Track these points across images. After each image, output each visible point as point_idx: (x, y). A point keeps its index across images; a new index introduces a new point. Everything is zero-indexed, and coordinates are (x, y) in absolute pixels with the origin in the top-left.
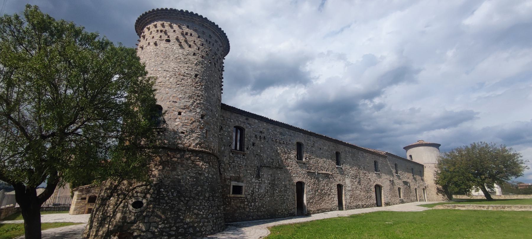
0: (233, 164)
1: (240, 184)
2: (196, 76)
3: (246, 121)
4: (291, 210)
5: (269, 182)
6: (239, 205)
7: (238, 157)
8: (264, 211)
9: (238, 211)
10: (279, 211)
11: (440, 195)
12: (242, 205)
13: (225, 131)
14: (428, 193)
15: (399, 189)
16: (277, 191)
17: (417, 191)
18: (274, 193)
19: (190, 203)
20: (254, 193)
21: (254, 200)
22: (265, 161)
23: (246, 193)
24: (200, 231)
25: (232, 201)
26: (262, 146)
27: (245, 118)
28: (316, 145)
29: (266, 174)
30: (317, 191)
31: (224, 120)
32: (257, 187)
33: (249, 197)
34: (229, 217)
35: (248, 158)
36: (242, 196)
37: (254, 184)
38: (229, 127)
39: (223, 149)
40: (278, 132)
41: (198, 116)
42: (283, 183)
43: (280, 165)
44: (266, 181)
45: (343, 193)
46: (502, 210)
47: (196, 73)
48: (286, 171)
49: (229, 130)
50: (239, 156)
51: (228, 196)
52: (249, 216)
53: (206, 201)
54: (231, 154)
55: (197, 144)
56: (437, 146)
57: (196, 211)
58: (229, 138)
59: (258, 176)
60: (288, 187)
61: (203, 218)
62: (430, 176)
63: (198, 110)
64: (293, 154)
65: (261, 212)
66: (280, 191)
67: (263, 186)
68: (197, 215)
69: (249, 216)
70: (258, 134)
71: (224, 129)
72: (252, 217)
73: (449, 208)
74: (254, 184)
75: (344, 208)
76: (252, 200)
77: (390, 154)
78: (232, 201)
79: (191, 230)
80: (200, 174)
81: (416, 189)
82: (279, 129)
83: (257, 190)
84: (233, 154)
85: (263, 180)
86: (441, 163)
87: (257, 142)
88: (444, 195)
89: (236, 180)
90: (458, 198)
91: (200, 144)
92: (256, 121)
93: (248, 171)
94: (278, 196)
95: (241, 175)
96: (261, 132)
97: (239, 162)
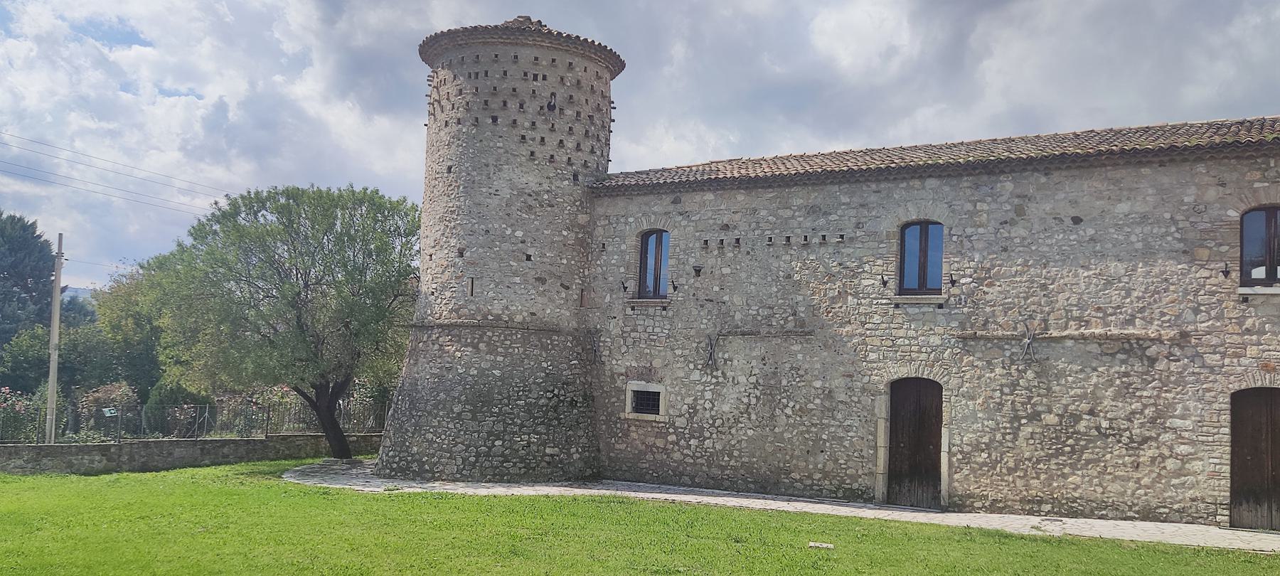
0: (633, 335)
1: (653, 387)
2: (450, 168)
3: (671, 208)
4: (854, 478)
5: (753, 379)
6: (650, 440)
7: (647, 315)
8: (734, 468)
9: (649, 457)
10: (796, 475)
12: (660, 443)
13: (613, 253)
16: (788, 411)
18: (773, 417)
19: (423, 420)
20: (696, 412)
21: (698, 433)
22: (738, 316)
23: (671, 412)
24: (431, 471)
25: (633, 428)
26: (726, 271)
27: (668, 199)
28: (1032, 209)
29: (742, 361)
30: (1035, 417)
31: (610, 223)
32: (708, 395)
33: (680, 422)
34: (624, 468)
35: (677, 314)
36: (658, 418)
37: (700, 387)
38: (623, 240)
39: (608, 299)
40: (799, 209)
41: (453, 255)
42: (818, 384)
43: (803, 324)
44: (742, 379)
47: (450, 163)
48: (834, 344)
49: (623, 247)
50: (651, 311)
51: (622, 415)
52: (682, 474)
53: (453, 419)
54: (629, 311)
55: (451, 311)
57: (430, 436)
58: (622, 270)
59: (711, 364)
60: (842, 397)
61: (442, 449)
63: (453, 242)
64: (877, 273)
65: (723, 468)
66: (803, 411)
67: (731, 393)
68: (431, 442)
69: (682, 474)
70: (714, 238)
71: (610, 249)
72: (692, 478)
74: (700, 387)
76: (692, 431)
78: (633, 428)
79: (415, 467)
80: (449, 369)
82: (799, 198)
83: (708, 405)
84: (633, 309)
85: (729, 374)
87: (710, 261)
89: (640, 377)
91: (457, 311)
92: (709, 196)
93: (678, 352)
94: (794, 426)
95: (657, 363)
96: (726, 227)
97: (650, 329)
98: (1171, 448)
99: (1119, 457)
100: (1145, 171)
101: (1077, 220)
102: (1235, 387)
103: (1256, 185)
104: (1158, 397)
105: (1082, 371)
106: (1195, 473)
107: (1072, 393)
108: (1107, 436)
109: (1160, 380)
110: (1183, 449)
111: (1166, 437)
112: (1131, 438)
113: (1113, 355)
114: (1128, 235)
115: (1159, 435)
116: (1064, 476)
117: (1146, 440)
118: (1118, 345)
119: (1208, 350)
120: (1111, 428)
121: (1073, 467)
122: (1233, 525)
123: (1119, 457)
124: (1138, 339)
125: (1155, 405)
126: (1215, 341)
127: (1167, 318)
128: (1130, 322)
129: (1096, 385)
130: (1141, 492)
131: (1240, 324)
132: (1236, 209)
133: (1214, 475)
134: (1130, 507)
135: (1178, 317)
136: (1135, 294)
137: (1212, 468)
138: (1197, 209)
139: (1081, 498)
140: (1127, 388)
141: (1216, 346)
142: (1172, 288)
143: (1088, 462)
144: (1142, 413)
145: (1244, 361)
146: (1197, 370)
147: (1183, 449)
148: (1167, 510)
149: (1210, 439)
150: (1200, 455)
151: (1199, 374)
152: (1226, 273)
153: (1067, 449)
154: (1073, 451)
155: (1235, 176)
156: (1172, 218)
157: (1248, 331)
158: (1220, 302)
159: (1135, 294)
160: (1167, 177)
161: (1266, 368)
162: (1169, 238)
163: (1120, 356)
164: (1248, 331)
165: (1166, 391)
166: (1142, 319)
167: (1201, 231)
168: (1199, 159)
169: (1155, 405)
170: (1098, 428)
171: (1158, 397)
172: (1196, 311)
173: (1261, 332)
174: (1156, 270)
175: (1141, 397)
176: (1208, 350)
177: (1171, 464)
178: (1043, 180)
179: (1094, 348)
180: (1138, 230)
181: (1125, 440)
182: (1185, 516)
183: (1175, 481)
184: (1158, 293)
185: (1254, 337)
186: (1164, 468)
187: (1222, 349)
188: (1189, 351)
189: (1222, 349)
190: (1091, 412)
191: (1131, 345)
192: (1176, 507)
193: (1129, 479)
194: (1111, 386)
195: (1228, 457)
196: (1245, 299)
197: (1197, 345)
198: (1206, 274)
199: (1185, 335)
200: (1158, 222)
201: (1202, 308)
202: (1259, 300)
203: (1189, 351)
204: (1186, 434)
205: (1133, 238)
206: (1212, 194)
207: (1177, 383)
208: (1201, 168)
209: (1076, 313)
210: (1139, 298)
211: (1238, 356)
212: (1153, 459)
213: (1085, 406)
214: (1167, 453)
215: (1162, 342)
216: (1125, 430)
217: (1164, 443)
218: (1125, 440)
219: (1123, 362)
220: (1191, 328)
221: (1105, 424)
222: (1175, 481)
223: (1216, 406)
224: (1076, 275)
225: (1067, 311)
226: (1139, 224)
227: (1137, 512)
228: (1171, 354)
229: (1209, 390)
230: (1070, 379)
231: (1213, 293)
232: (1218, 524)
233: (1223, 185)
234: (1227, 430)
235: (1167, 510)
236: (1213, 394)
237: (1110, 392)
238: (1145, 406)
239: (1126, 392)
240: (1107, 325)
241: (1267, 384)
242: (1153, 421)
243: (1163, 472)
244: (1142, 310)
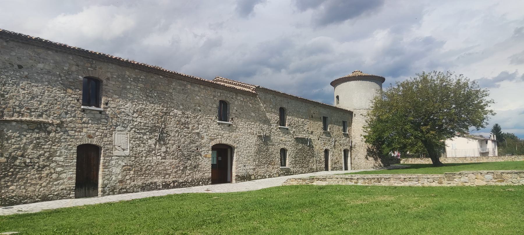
11: (371, 159)
14: (353, 156)
15: (283, 152)
17: (330, 154)
45: (102, 161)
46: (377, 184)
56: (379, 80)
62: (359, 129)
73: (304, 183)
75: (100, 193)
77: (265, 91)
81: (326, 152)
86: (380, 106)
88: (376, 160)
90: (410, 163)
98: (54, 169)
99: (33, 175)
100: (50, 52)
101: (20, 67)
102: (79, 144)
103: (89, 69)
104: (51, 148)
105: (19, 137)
106: (63, 179)
107: (14, 147)
108: (28, 166)
109: (52, 141)
110: (59, 169)
111: (53, 165)
112: (39, 167)
113: (33, 130)
114: (42, 78)
115: (50, 164)
116: (8, 187)
117: (44, 166)
118: (34, 126)
119: (70, 129)
120: (31, 162)
121: (12, 182)
122: (76, 197)
123: (33, 175)
124: (44, 123)
125: (49, 151)
126: (73, 126)
127: (56, 115)
128: (41, 116)
129: (25, 143)
130: (42, 189)
131: (81, 120)
132: (82, 76)
133: (70, 178)
134: (37, 196)
135: (60, 115)
136: (44, 104)
137: (69, 176)
138: (69, 73)
139: (15, 196)
140: (38, 144)
141: (73, 128)
142: (58, 103)
143: (19, 178)
144: (44, 155)
145: (82, 134)
146: (66, 137)
147: (59, 169)
148: (52, 196)
149: (69, 164)
150: (65, 171)
151: (67, 138)
152: (78, 100)
153: (10, 174)
154: (12, 175)
155: (82, 63)
156: (59, 74)
157: (84, 123)
158: (75, 110)
159: (44, 104)
160: (58, 57)
161: (90, 137)
162: (58, 83)
163: (37, 131)
164: (84, 123)
165: (54, 146)
166: (46, 115)
167: (70, 82)
168: (71, 54)
169: (49, 151)
170: (25, 163)
171: (51, 148)
172: (66, 113)
173: (88, 123)
174: (53, 95)
175: (44, 148)
176: (70, 129)
177: (54, 176)
178: (5, 44)
179: (25, 126)
180: (46, 77)
181: (36, 167)
182: (60, 197)
183: (56, 183)
184: (53, 104)
185: (86, 125)
186: (52, 178)
187: (75, 129)
188: (63, 129)
189: (75, 129)
190: (22, 156)
191: (41, 126)
192: (55, 193)
193: (37, 184)
194: (32, 143)
195: (75, 171)
196: (84, 110)
197: (66, 127)
198: (71, 99)
199: (62, 122)
200: (54, 75)
201: (69, 112)
202: (88, 112)
203: (63, 129)
204: (61, 163)
205: (44, 80)
206: (74, 68)
207: (58, 142)
208: (71, 57)
209: (18, 109)
210: (45, 106)
211: (80, 132)
212: (48, 174)
213: (19, 153)
214: (53, 171)
215: (53, 125)
216: (37, 163)
217: (52, 168)
218: (36, 167)
219: (37, 133)
220: (64, 120)
221: (28, 161)
222: (56, 183)
223: (72, 151)
224: (19, 92)
225: (14, 108)
226: (46, 74)
227: (40, 198)
228: (57, 130)
229: (70, 145)
230: (13, 140)
231: (73, 107)
232: (71, 198)
233: (78, 66)
234: (75, 160)
235: (52, 196)
236: (71, 146)
237: (31, 147)
238: (45, 152)
239: (37, 146)
240: (31, 116)
241: (89, 142)
242: (48, 158)
243: (51, 180)
244: (46, 111)
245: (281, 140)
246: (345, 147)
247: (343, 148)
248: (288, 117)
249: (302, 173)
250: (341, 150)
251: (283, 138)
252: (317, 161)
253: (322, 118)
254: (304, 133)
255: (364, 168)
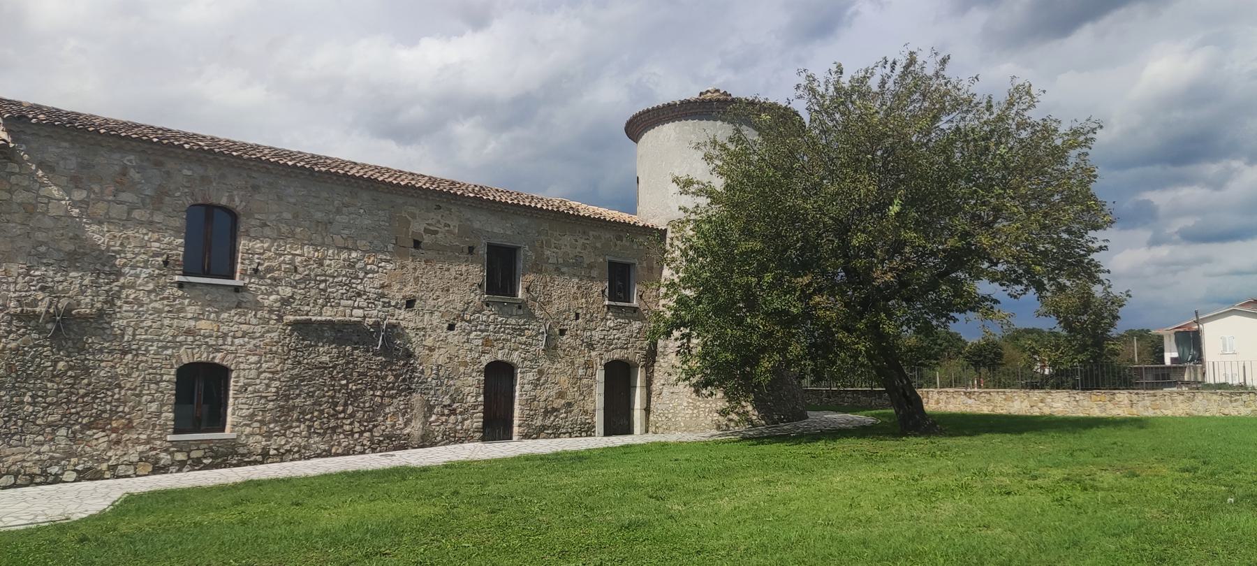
14: (656, 386)
245: (189, 332)
246: (617, 355)
247: (599, 359)
248: (243, 244)
249: (328, 454)
250: (588, 365)
251: (203, 325)
252: (431, 409)
253: (482, 251)
254: (361, 301)
255: (687, 429)
